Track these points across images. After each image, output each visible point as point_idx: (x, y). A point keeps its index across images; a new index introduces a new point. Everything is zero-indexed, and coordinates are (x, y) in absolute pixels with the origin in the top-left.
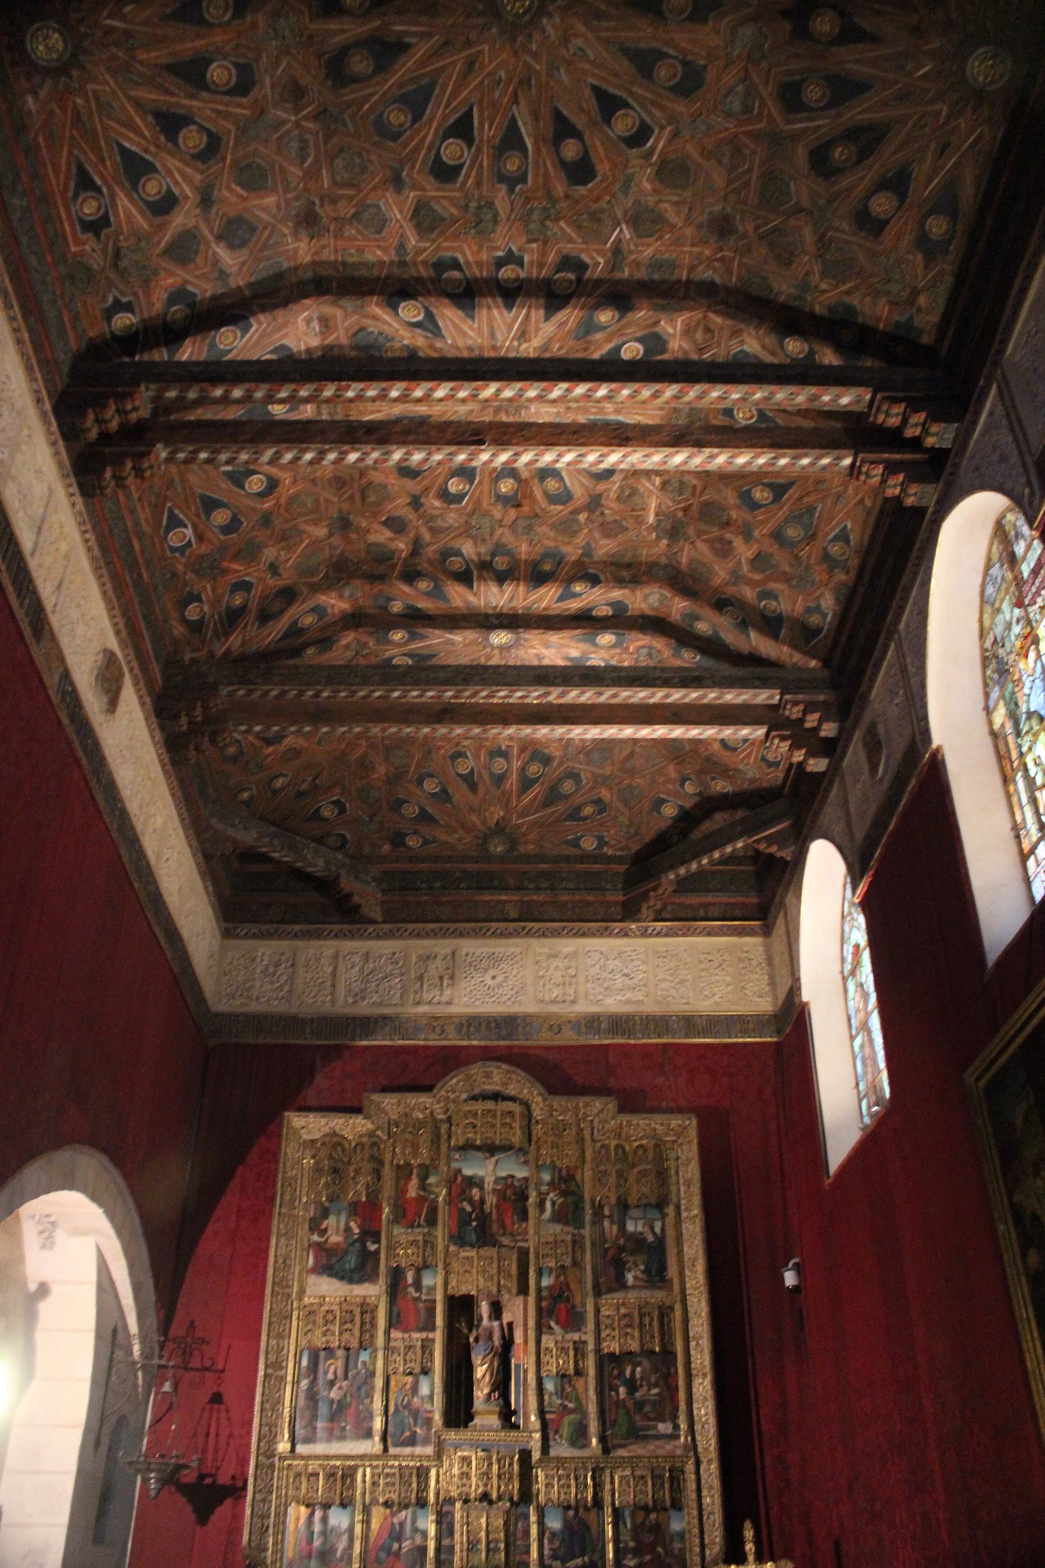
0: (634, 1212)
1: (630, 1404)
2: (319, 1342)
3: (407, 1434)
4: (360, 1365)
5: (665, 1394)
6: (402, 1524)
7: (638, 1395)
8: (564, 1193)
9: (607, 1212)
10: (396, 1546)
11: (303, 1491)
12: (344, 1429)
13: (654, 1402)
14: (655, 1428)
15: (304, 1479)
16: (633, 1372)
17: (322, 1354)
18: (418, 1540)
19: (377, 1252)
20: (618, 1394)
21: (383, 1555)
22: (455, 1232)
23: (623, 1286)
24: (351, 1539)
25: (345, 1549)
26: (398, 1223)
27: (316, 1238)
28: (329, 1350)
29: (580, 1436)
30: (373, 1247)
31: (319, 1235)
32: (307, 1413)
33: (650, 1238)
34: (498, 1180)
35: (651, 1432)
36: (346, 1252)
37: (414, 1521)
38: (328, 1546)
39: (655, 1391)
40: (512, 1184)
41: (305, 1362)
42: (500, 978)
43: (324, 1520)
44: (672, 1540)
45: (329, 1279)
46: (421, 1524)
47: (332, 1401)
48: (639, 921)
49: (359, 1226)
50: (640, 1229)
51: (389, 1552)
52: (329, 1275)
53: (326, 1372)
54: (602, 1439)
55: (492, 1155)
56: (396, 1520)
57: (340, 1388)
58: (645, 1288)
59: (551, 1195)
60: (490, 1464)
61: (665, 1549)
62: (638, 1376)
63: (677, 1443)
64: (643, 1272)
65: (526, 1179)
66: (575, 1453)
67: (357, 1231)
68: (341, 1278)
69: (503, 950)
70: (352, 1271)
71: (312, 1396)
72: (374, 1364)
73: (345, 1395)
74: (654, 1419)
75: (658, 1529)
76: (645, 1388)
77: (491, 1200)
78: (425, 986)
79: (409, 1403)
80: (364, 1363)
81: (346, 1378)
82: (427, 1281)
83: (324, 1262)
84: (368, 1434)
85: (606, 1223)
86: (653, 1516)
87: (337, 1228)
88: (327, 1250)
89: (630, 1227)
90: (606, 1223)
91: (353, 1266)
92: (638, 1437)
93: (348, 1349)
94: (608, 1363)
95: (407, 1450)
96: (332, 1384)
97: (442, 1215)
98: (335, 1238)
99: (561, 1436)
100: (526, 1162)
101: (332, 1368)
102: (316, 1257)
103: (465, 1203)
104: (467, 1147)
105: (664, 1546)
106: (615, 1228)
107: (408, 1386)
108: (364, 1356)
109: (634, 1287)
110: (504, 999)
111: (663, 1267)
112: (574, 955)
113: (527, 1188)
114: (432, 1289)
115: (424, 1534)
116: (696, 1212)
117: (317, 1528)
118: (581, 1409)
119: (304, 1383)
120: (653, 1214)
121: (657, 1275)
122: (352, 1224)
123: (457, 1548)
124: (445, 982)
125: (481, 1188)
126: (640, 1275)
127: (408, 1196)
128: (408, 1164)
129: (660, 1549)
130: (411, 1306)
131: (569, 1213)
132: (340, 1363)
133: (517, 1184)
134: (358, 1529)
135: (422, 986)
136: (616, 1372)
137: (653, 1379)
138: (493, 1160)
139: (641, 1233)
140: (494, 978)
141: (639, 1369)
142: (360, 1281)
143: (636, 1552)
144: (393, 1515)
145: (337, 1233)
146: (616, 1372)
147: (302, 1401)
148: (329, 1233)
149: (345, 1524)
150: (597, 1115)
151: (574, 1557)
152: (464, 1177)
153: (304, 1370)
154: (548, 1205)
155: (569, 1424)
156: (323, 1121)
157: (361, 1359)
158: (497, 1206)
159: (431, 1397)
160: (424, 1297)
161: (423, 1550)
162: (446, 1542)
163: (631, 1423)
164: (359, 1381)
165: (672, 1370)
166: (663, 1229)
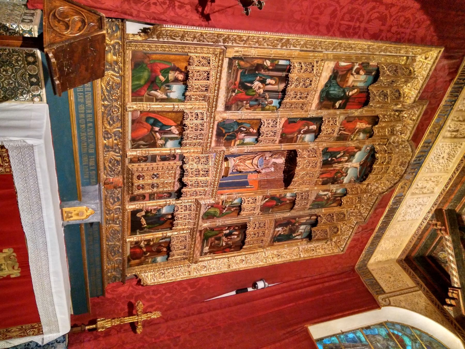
0: (309, 227)
1: (220, 235)
2: (293, 76)
3: (224, 132)
4: (270, 100)
5: (222, 248)
6: (170, 132)
7: (224, 238)
8: (328, 199)
9: (312, 218)
10: (157, 129)
11: (198, 68)
12: (234, 91)
13: (219, 244)
14: (207, 246)
15: (206, 69)
16: (234, 235)
17: (284, 74)
18: (160, 142)
19: (334, 107)
20: (226, 230)
21: (152, 121)
22: (330, 150)
23: (276, 227)
24: (162, 100)
25: (156, 96)
26: (346, 118)
27: (357, 66)
28: (286, 79)
29: (208, 216)
30: (337, 105)
31: (357, 69)
32: (248, 65)
33: (294, 235)
34: (347, 169)
35: (205, 244)
36: (340, 87)
37: (172, 139)
38: (159, 85)
39: (224, 244)
40: (342, 176)
41: (282, 62)
42: (441, 161)
43: (176, 80)
44: (152, 258)
45: (328, 76)
46: (170, 144)
47: (252, 82)
48: (432, 217)
49: (353, 95)
50: (300, 231)
51: (154, 125)
52: (331, 77)
53: (272, 77)
54: (206, 229)
55: (361, 165)
56: (173, 128)
57: (259, 88)
58: (273, 236)
59: (330, 194)
60: (203, 187)
61: (148, 256)
62: (232, 237)
63: (198, 254)
64: (280, 234)
65: (342, 183)
66: (201, 216)
67: (350, 94)
68: (326, 85)
69: (454, 161)
70: (328, 93)
71: (259, 67)
72: (268, 110)
73: (255, 91)
74: (211, 245)
75: (159, 252)
76: (226, 240)
77: (338, 166)
78: (459, 123)
79: (242, 132)
80: (271, 103)
81: (265, 91)
82: (308, 137)
83: (340, 73)
84: (228, 108)
85: (308, 218)
86: (165, 249)
87: (357, 80)
88: (346, 74)
89: (302, 227)
90: (308, 218)
91: (331, 92)
92: (204, 240)
93: (284, 92)
94: (243, 227)
95: (215, 133)
96: (263, 82)
97: (341, 143)
98: (351, 80)
99: (209, 208)
100: (350, 182)
101: (273, 82)
102: (344, 67)
103: (342, 154)
104: (372, 156)
105: (149, 256)
106: (304, 221)
107: (251, 130)
108: (275, 102)
109: (274, 231)
110: (431, 163)
111: (279, 240)
112: (432, 192)
113: (338, 183)
114: (303, 139)
115: (163, 145)
116: (302, 256)
117: (172, 75)
118: (222, 215)
119: (268, 63)
120: (305, 235)
121: (278, 239)
122: (356, 90)
123: (154, 164)
124: (454, 133)
125: (346, 161)
126: (279, 233)
127: (358, 123)
128: (376, 123)
129: (148, 254)
130: (296, 129)
131: (319, 202)
132: (276, 87)
133: (342, 177)
134: (168, 106)
135: (460, 121)
136: (237, 228)
137: (229, 243)
138: (358, 166)
139: (298, 231)
140: (443, 158)
141: (236, 237)
142: (321, 97)
143: (147, 246)
144: (176, 126)
145: (354, 81)
146: (237, 228)
147: (256, 62)
148: (356, 76)
149: (173, 95)
150: (360, 212)
151: (146, 220)
152: (356, 152)
153: (276, 62)
154: (326, 193)
155: (216, 211)
156: (425, 73)
157: (274, 101)
158: (334, 170)
159: (243, 144)
160: (299, 136)
161: (154, 145)
162: (158, 158)
163: (211, 237)
164: (261, 100)
165: (232, 249)
166: (297, 239)
